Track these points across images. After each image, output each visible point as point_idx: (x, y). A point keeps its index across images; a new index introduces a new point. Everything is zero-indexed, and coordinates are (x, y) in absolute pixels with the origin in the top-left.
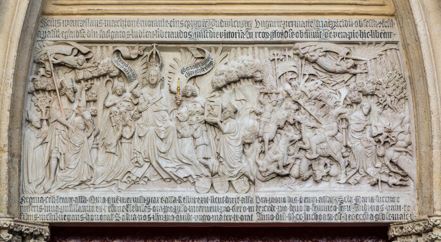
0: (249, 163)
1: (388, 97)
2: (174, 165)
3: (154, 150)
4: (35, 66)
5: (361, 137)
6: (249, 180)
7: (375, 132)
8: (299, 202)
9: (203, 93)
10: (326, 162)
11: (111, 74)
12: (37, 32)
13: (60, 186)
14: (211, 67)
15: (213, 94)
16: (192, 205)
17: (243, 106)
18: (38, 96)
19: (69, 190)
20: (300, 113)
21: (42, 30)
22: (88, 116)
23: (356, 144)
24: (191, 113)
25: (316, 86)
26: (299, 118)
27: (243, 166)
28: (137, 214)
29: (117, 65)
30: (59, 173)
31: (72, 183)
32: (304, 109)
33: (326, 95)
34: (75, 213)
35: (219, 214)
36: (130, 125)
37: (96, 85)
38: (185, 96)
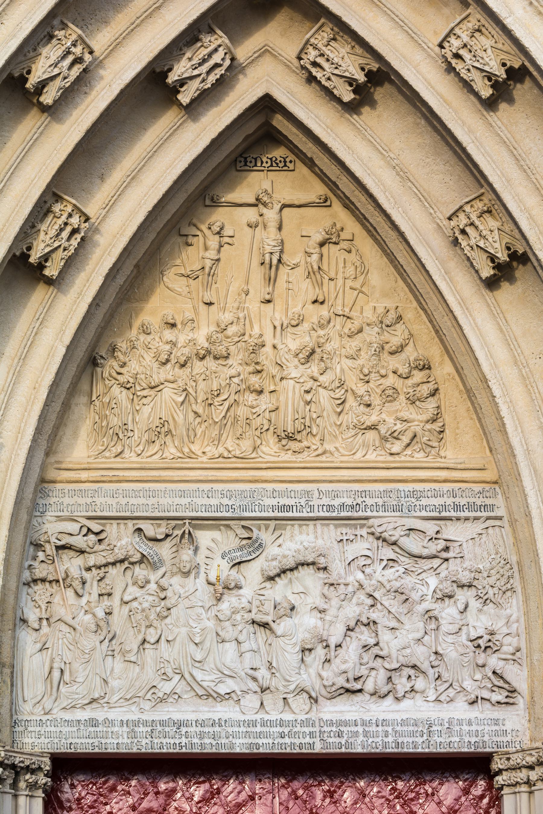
0: (309, 675)
1: (490, 588)
2: (213, 677)
3: (186, 658)
4: (32, 549)
6: (310, 697)
7: (474, 634)
8: (374, 725)
9: (250, 584)
10: (410, 673)
11: (130, 559)
12: (35, 505)
13: (64, 705)
15: (262, 586)
16: (236, 729)
17: (301, 601)
18: (36, 588)
19: (76, 710)
20: (376, 610)
21: (41, 502)
22: (101, 614)
25: (397, 574)
26: (374, 615)
27: (302, 679)
28: (164, 741)
29: (138, 548)
30: (63, 689)
31: (80, 701)
32: (381, 604)
33: (410, 586)
34: (83, 741)
35: (271, 741)
36: (155, 625)
37: (111, 574)
38: (227, 588)
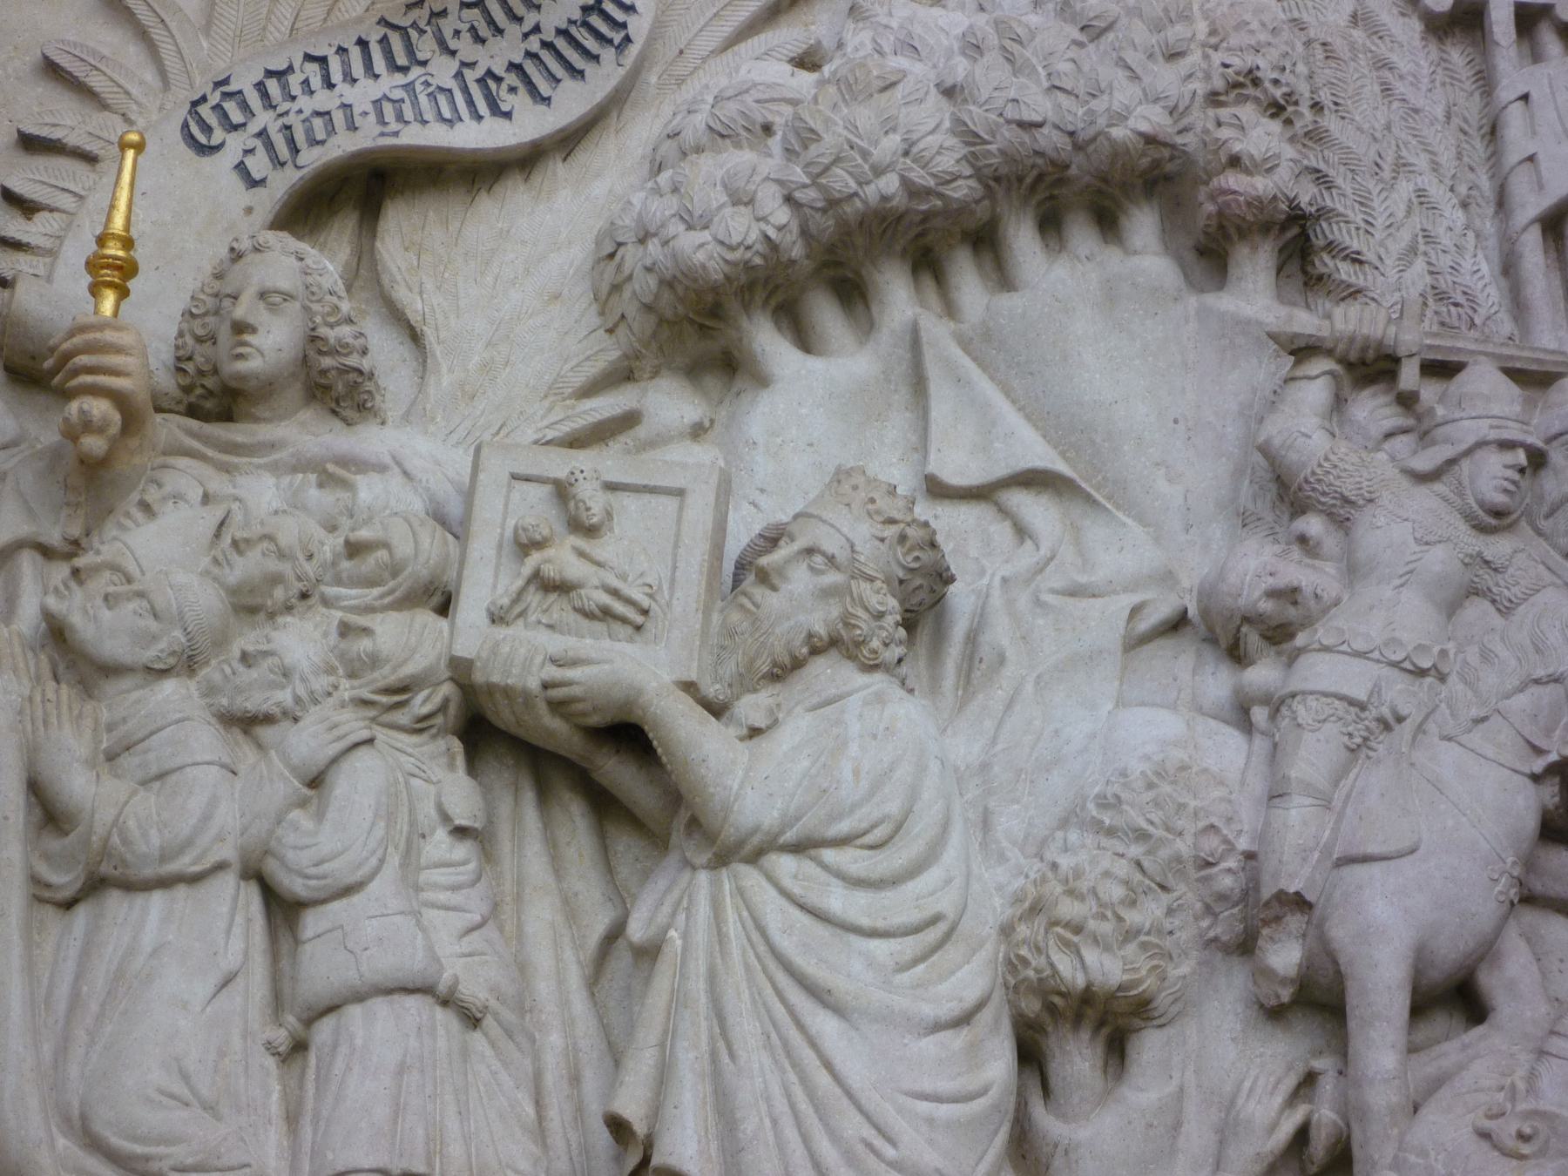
14: (604, 78)
17: (1027, 557)
24: (273, 565)
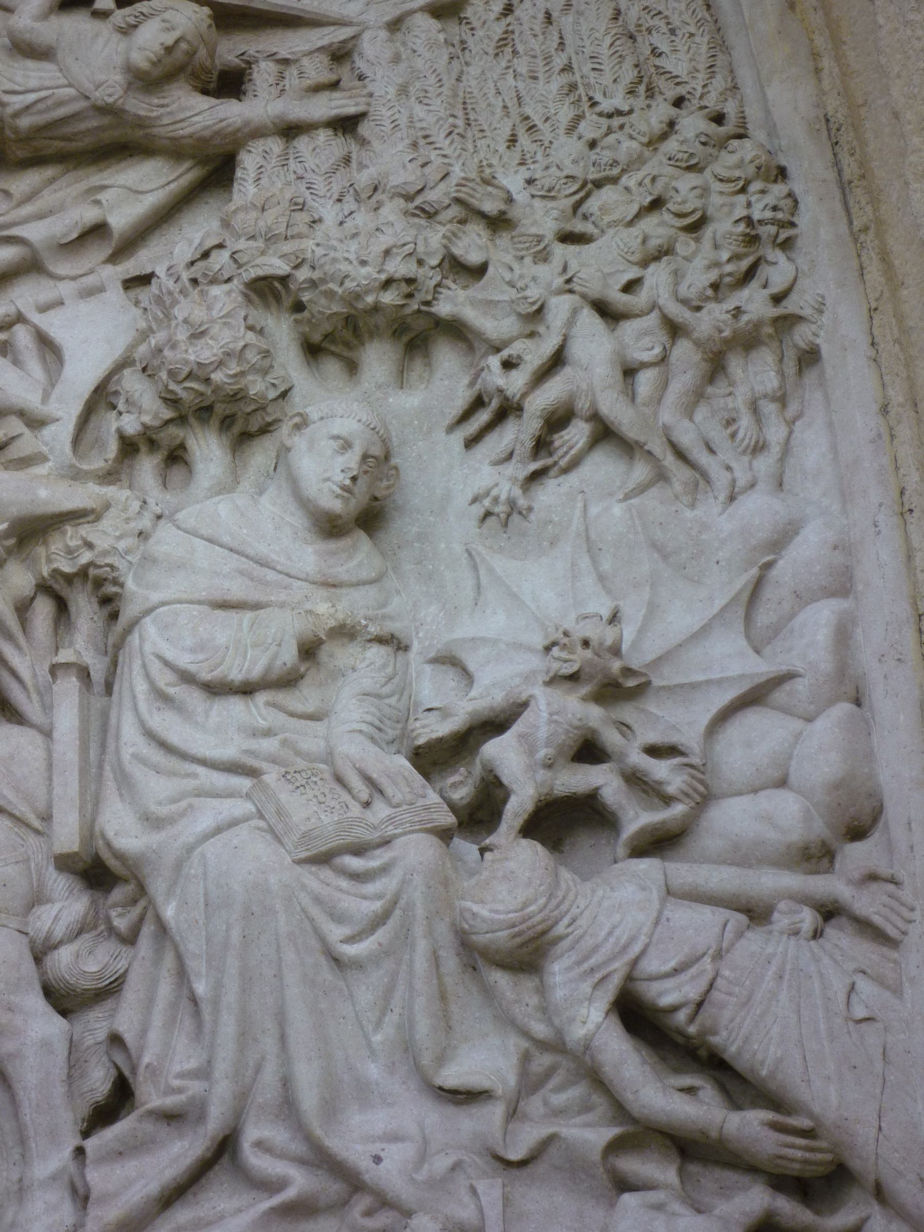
1: (589, 319)
5: (269, 745)
23: (204, 821)
